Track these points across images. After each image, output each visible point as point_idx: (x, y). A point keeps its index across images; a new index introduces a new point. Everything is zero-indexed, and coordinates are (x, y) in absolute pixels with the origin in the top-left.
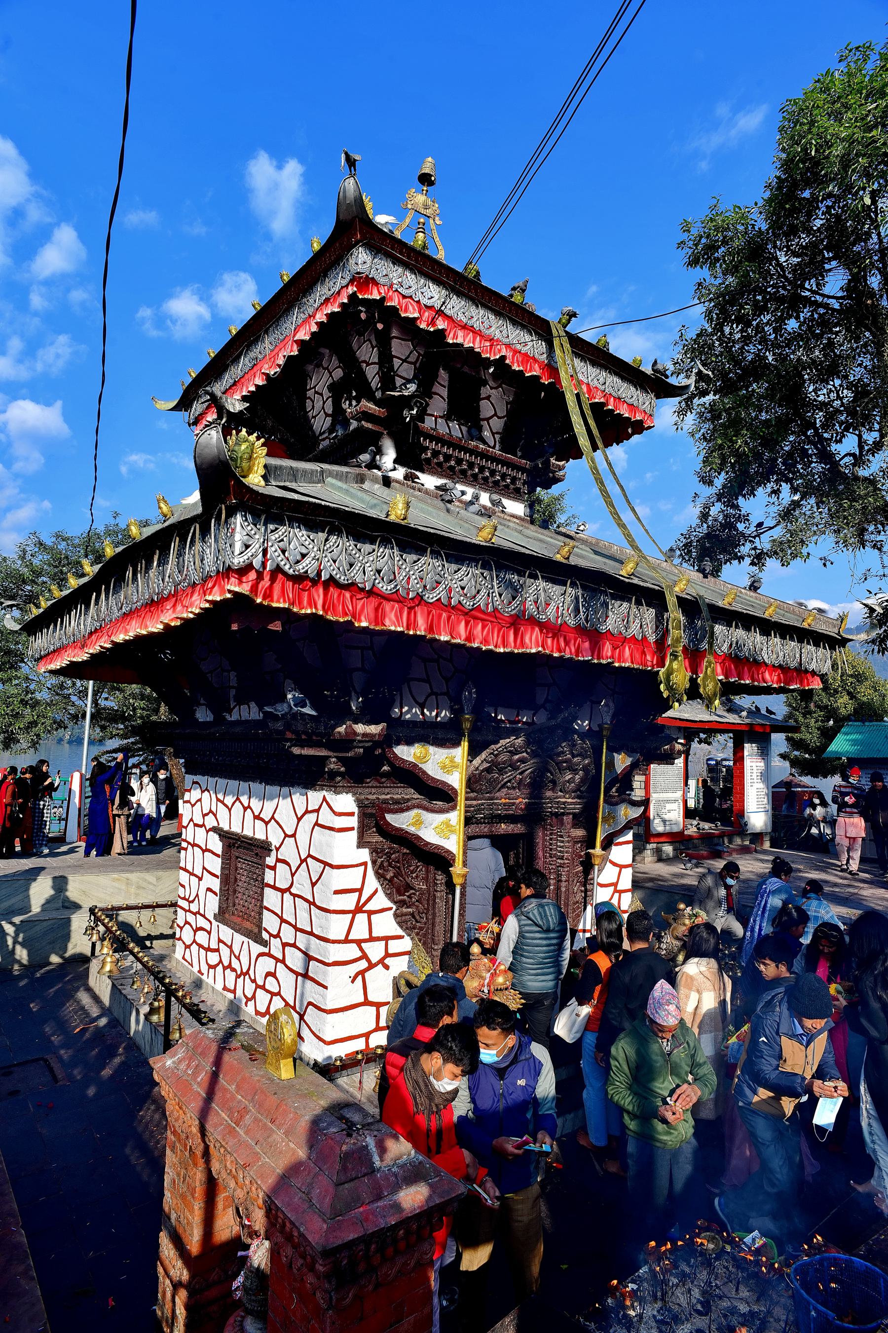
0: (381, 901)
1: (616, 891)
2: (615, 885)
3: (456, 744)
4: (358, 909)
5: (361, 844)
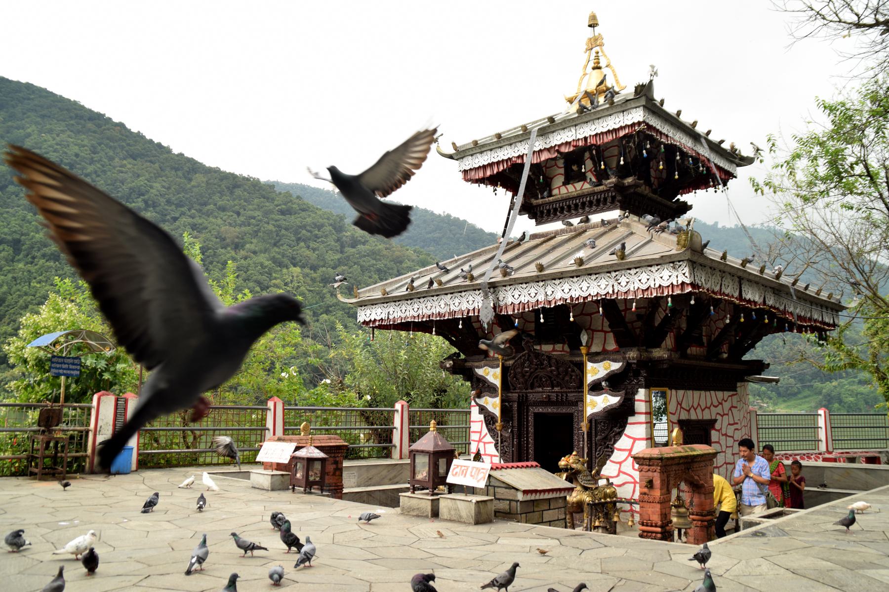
0: (489, 438)
1: (630, 454)
2: (630, 450)
3: (498, 367)
4: (479, 441)
5: (480, 413)
